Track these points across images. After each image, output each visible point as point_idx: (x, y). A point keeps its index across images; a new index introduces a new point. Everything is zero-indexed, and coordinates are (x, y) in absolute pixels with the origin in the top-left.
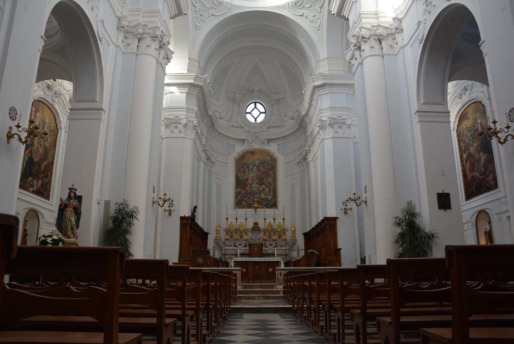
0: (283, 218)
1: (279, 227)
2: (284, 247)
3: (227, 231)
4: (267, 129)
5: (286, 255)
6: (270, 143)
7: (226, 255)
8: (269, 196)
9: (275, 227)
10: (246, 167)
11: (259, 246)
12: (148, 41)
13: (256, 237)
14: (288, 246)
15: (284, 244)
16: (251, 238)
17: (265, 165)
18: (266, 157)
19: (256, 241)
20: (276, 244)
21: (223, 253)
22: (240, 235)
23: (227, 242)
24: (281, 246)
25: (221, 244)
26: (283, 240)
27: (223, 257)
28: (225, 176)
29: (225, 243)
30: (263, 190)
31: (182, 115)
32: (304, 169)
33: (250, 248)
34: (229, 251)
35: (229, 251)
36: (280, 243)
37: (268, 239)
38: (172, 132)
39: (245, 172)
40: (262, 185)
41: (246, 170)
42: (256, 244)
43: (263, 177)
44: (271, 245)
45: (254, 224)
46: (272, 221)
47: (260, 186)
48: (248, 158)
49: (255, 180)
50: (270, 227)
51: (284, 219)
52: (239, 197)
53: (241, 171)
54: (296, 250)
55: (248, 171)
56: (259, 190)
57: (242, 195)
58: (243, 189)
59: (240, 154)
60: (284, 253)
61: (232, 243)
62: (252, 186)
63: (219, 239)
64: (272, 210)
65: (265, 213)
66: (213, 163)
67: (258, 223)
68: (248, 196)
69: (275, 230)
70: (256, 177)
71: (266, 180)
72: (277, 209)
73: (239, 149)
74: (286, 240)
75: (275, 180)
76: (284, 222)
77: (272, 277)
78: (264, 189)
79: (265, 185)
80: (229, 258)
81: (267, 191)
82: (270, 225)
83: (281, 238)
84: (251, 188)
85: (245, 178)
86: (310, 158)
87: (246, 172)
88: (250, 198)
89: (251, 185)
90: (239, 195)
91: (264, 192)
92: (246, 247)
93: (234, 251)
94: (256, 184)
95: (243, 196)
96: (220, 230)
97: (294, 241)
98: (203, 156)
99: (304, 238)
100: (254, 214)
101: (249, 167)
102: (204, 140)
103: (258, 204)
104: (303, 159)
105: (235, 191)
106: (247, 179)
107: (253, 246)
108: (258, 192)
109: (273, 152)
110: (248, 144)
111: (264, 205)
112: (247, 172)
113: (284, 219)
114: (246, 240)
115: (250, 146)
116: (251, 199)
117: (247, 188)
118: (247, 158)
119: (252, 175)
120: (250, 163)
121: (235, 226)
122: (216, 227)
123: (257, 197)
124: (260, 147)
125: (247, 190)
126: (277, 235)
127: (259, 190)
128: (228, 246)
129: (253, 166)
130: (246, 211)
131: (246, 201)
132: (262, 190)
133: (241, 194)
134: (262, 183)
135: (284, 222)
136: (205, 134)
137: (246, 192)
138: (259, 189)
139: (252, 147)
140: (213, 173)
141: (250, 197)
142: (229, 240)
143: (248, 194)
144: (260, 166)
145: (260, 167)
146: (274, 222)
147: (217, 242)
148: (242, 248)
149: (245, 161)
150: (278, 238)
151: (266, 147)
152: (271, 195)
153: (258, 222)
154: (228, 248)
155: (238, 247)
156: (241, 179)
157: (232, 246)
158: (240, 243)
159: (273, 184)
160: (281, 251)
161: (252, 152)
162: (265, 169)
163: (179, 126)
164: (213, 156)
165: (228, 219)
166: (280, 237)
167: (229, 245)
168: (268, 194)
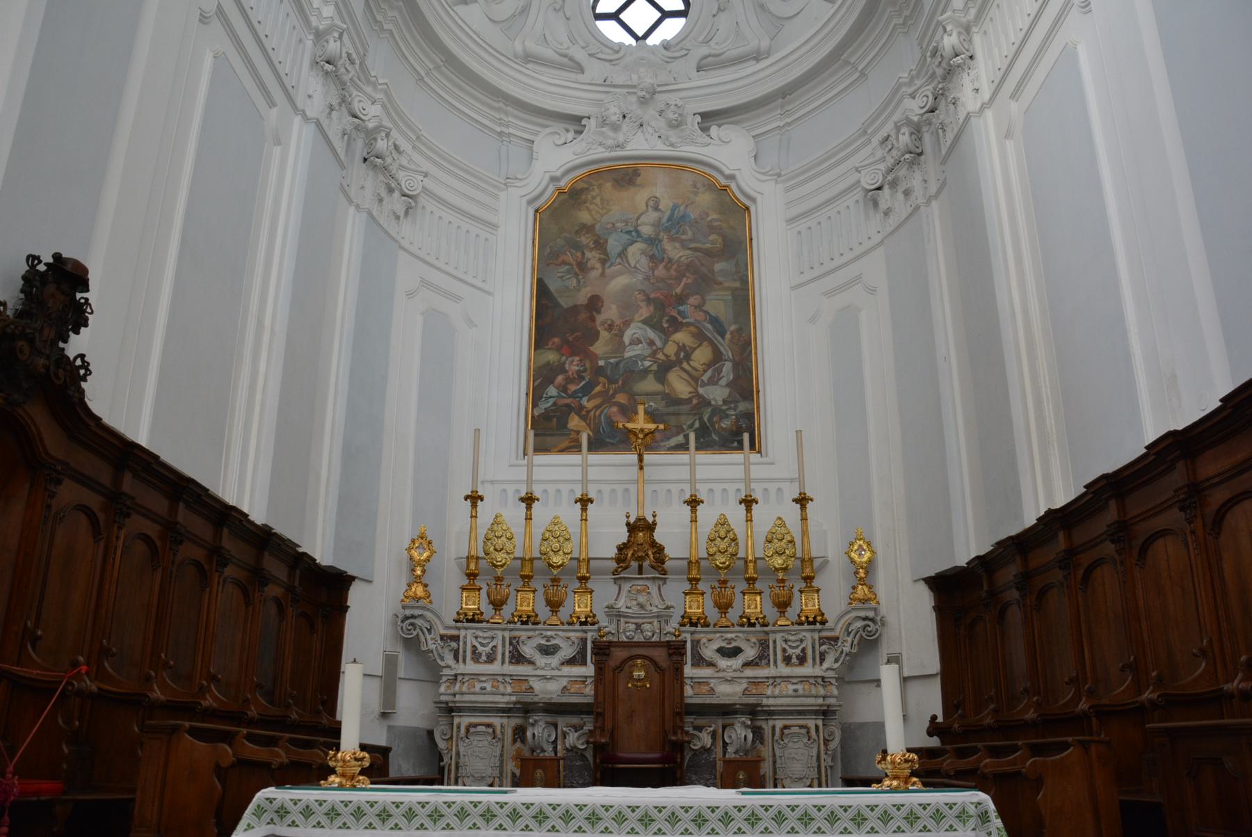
0: (796, 496)
1: (777, 545)
2: (810, 660)
5: (826, 713)
6: (714, 130)
7: (460, 710)
8: (716, 383)
9: (753, 545)
11: (660, 655)
13: (642, 606)
14: (836, 661)
15: (808, 644)
16: (610, 607)
17: (690, 233)
18: (696, 194)
19: (638, 626)
20: (764, 645)
21: (443, 698)
22: (546, 593)
23: (469, 636)
24: (794, 660)
25: (431, 643)
26: (801, 624)
27: (443, 721)
28: (480, 284)
29: (456, 638)
30: (682, 354)
33: (600, 669)
34: (478, 686)
35: (478, 686)
36: (786, 641)
37: (713, 614)
39: (583, 267)
40: (676, 331)
41: (592, 257)
42: (638, 645)
43: (678, 290)
44: (734, 652)
45: (632, 528)
46: (736, 515)
47: (666, 334)
48: (602, 200)
50: (723, 545)
51: (802, 501)
52: (552, 391)
53: (564, 263)
55: (603, 262)
56: (660, 356)
57: (569, 380)
58: (573, 354)
59: (562, 184)
61: (500, 639)
62: (622, 337)
64: (737, 457)
65: (693, 472)
67: (654, 524)
68: (598, 388)
69: (751, 565)
70: (642, 292)
71: (698, 307)
72: (759, 452)
74: (817, 620)
75: (743, 302)
76: (804, 519)
78: (685, 353)
80: (478, 733)
81: (704, 360)
82: (722, 533)
83: (792, 612)
84: (621, 347)
85: (582, 298)
87: (593, 268)
88: (613, 396)
89: (617, 331)
90: (550, 381)
91: (685, 365)
92: (584, 663)
93: (509, 690)
94: (640, 325)
95: (572, 388)
96: (428, 560)
97: (872, 627)
99: (938, 609)
100: (630, 482)
101: (606, 241)
103: (652, 416)
105: (529, 361)
106: (595, 304)
107: (619, 655)
108: (655, 368)
109: (727, 172)
110: (602, 134)
112: (598, 265)
113: (802, 501)
114: (582, 624)
115: (610, 142)
117: (591, 348)
118: (598, 200)
120: (614, 225)
121: (518, 540)
122: (407, 543)
123: (647, 394)
124: (661, 149)
125: (596, 355)
126: (767, 592)
127: (660, 356)
128: (476, 656)
129: (627, 237)
130: (585, 466)
131: (588, 412)
133: (560, 378)
135: (804, 519)
137: (588, 365)
138: (661, 349)
139: (620, 146)
140: (401, 247)
141: (611, 392)
142: (481, 622)
143: (602, 379)
144: (662, 235)
146: (749, 520)
148: (556, 673)
149: (584, 217)
150: (771, 612)
152: (723, 382)
153: (654, 516)
154: (471, 667)
155: (531, 663)
156: (565, 302)
157: (499, 657)
158: (548, 639)
159: (733, 328)
160: (791, 687)
162: (689, 252)
164: (404, 162)
165: (481, 499)
166: (783, 606)
167: (480, 649)
168: (709, 373)
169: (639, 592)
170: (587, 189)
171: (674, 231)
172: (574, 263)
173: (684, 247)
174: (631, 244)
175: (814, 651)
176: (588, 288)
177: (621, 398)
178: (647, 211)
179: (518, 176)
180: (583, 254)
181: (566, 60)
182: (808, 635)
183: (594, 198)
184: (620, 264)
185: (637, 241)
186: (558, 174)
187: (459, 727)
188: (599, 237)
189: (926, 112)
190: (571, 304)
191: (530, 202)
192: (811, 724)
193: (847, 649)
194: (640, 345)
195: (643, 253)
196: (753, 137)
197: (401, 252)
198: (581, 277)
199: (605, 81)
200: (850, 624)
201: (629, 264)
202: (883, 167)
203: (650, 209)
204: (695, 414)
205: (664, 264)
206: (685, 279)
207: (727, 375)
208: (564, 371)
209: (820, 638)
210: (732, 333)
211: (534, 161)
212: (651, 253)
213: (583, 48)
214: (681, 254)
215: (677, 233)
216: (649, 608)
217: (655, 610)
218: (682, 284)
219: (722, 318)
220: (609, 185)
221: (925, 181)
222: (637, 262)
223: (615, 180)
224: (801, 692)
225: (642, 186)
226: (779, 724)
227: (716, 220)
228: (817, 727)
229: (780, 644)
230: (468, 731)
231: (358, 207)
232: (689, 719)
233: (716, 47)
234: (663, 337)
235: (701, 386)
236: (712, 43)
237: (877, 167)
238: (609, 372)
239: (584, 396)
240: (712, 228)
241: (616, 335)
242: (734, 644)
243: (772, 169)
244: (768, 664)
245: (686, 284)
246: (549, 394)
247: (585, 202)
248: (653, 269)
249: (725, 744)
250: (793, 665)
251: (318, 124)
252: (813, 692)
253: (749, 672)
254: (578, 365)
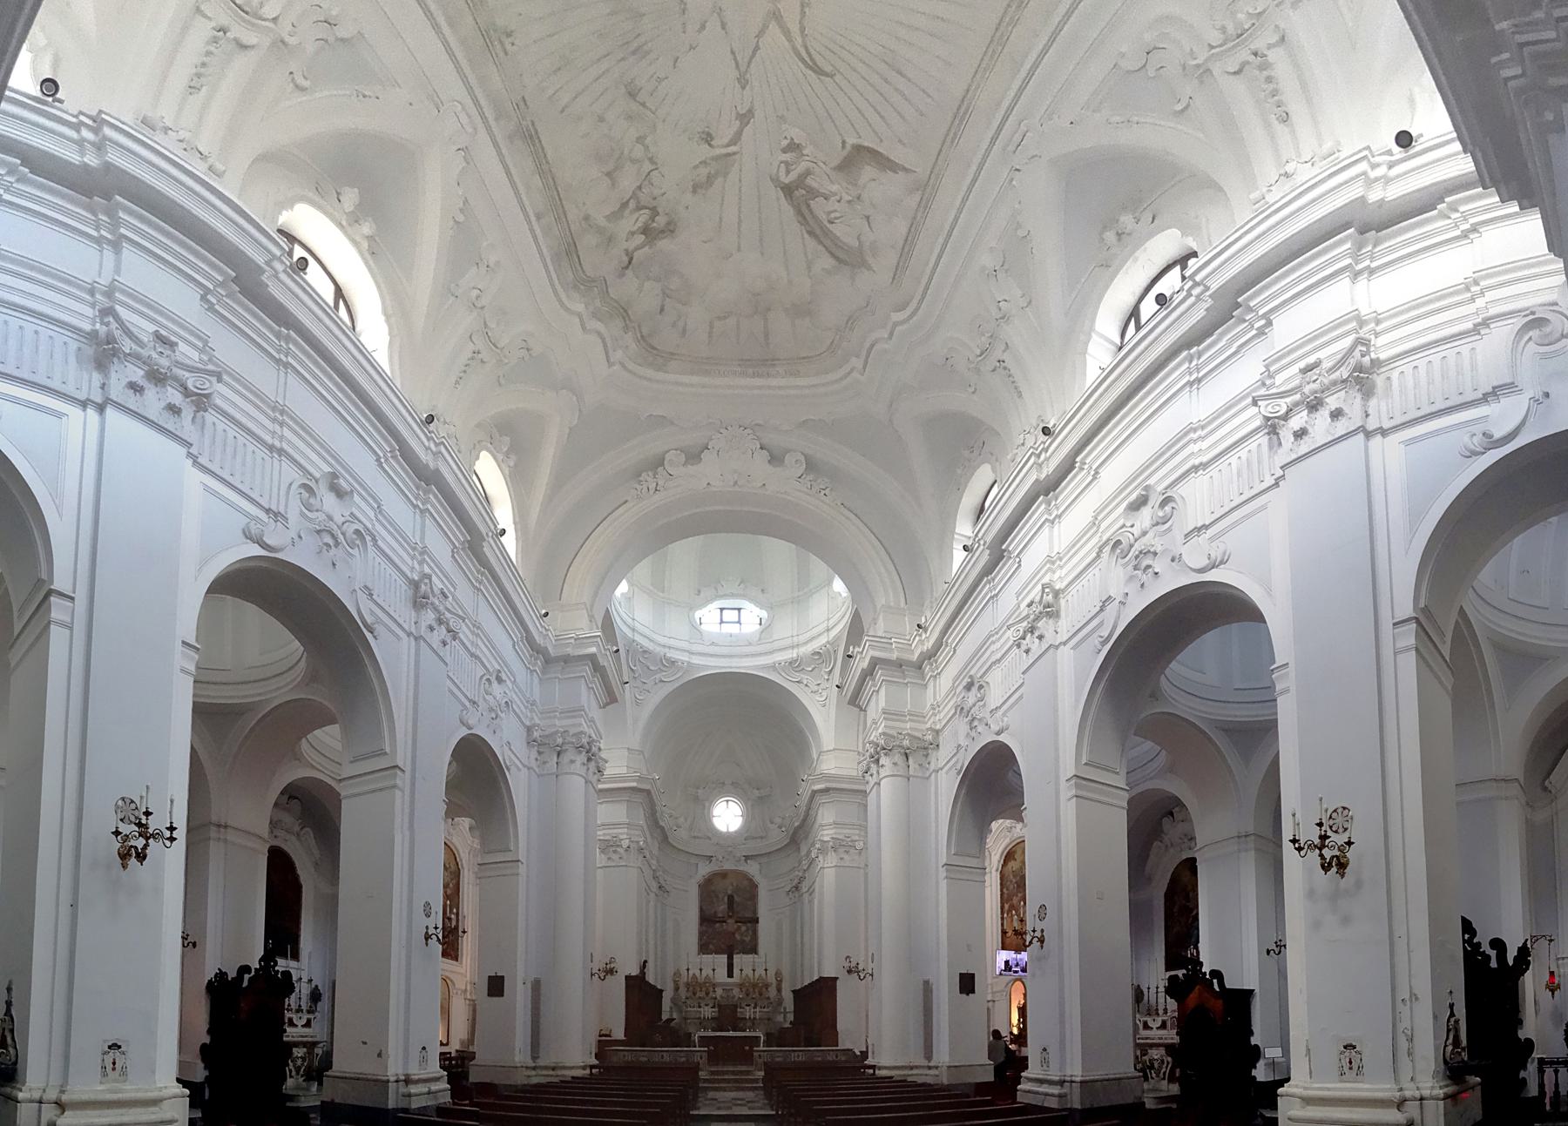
3: (688, 985)
12: (570, 755)
23: (688, 1002)
31: (622, 833)
38: (609, 859)
51: (766, 970)
64: (751, 956)
73: (705, 870)
77: (747, 1058)
85: (713, 912)
86: (804, 887)
98: (654, 885)
102: (654, 862)
136: (655, 852)
147: (673, 1000)
149: (713, 888)
161: (724, 875)
163: (618, 849)
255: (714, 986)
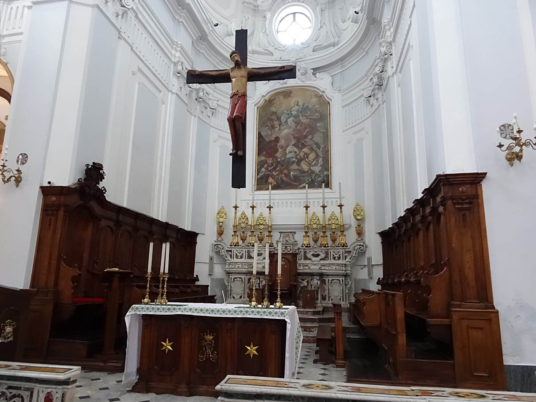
2: (341, 258)
4: (313, 52)
5: (346, 276)
7: (232, 273)
8: (317, 166)
10: (276, 119)
14: (350, 259)
18: (311, 99)
19: (286, 247)
20: (327, 253)
21: (227, 270)
22: (258, 237)
23: (235, 250)
24: (336, 258)
25: (223, 253)
29: (231, 251)
30: (306, 156)
32: (379, 105)
35: (237, 266)
36: (334, 252)
37: (312, 243)
39: (273, 127)
40: (304, 148)
43: (305, 134)
46: (319, 211)
47: (300, 149)
49: (291, 140)
52: (263, 170)
53: (267, 126)
54: (365, 266)
55: (280, 125)
56: (298, 157)
57: (268, 166)
59: (266, 98)
60: (341, 272)
63: (220, 244)
66: (211, 109)
68: (278, 168)
70: (292, 135)
71: (311, 139)
72: (331, 188)
74: (344, 245)
75: (326, 137)
79: (308, 148)
85: (273, 138)
87: (276, 127)
88: (283, 171)
89: (284, 148)
91: (306, 160)
93: (247, 267)
95: (270, 168)
97: (362, 248)
99: (382, 243)
104: (378, 85)
106: (277, 139)
108: (296, 161)
109: (322, 90)
111: (308, 182)
112: (278, 126)
113: (341, 206)
116: (284, 173)
117: (276, 155)
119: (286, 131)
120: (283, 112)
121: (250, 220)
123: (294, 170)
128: (237, 257)
129: (288, 116)
132: (303, 157)
133: (266, 165)
134: (303, 144)
137: (275, 161)
140: (211, 126)
141: (282, 170)
144: (300, 115)
145: (300, 116)
148: (262, 262)
149: (273, 109)
151: (310, 82)
152: (319, 165)
154: (235, 260)
156: (267, 140)
159: (323, 146)
160: (335, 267)
162: (308, 120)
164: (210, 97)
167: (238, 254)
169: (286, 236)
170: (275, 99)
171: (303, 113)
172: (270, 126)
173: (307, 118)
174: (289, 118)
175: (343, 256)
176: (275, 134)
177: (285, 171)
178: (294, 106)
179: (251, 96)
180: (273, 122)
181: (267, 52)
182: (341, 250)
183: (277, 102)
184: (285, 125)
185: (291, 117)
186: (264, 94)
187: (231, 279)
188: (278, 116)
189: (380, 72)
190: (269, 140)
191: (255, 105)
192: (341, 279)
193: (354, 255)
194: (292, 153)
195: (293, 121)
196: (331, 76)
197: (211, 128)
198: (272, 131)
199: (280, 59)
200: (355, 247)
201: (288, 125)
202: (371, 88)
203: (295, 105)
204: (310, 176)
205: (300, 125)
206: (307, 130)
207: (321, 163)
208: (267, 163)
209: (345, 251)
210: (322, 148)
211: (256, 91)
212: (295, 121)
213: (273, 46)
214: (306, 121)
215: (304, 113)
216: (289, 241)
217: (291, 242)
218: (306, 132)
219: (319, 143)
220: (282, 97)
221: (383, 95)
222: (291, 124)
223: (284, 96)
224: (337, 269)
225: (292, 97)
226: (331, 279)
227: (317, 108)
228: (342, 280)
229: (332, 253)
230: (234, 280)
231: (195, 116)
232: (300, 277)
233: (319, 42)
234: (299, 150)
235: (312, 167)
236: (318, 41)
237: (369, 89)
238: (281, 163)
239: (273, 171)
240: (316, 111)
241: (284, 150)
242: (317, 253)
243: (337, 88)
244: (328, 259)
245: (307, 132)
246: (262, 171)
247: (274, 104)
248: (296, 127)
249: (311, 285)
250: (336, 260)
251: (177, 94)
252: (341, 269)
253: (322, 262)
254: (271, 161)
255: (270, 229)
